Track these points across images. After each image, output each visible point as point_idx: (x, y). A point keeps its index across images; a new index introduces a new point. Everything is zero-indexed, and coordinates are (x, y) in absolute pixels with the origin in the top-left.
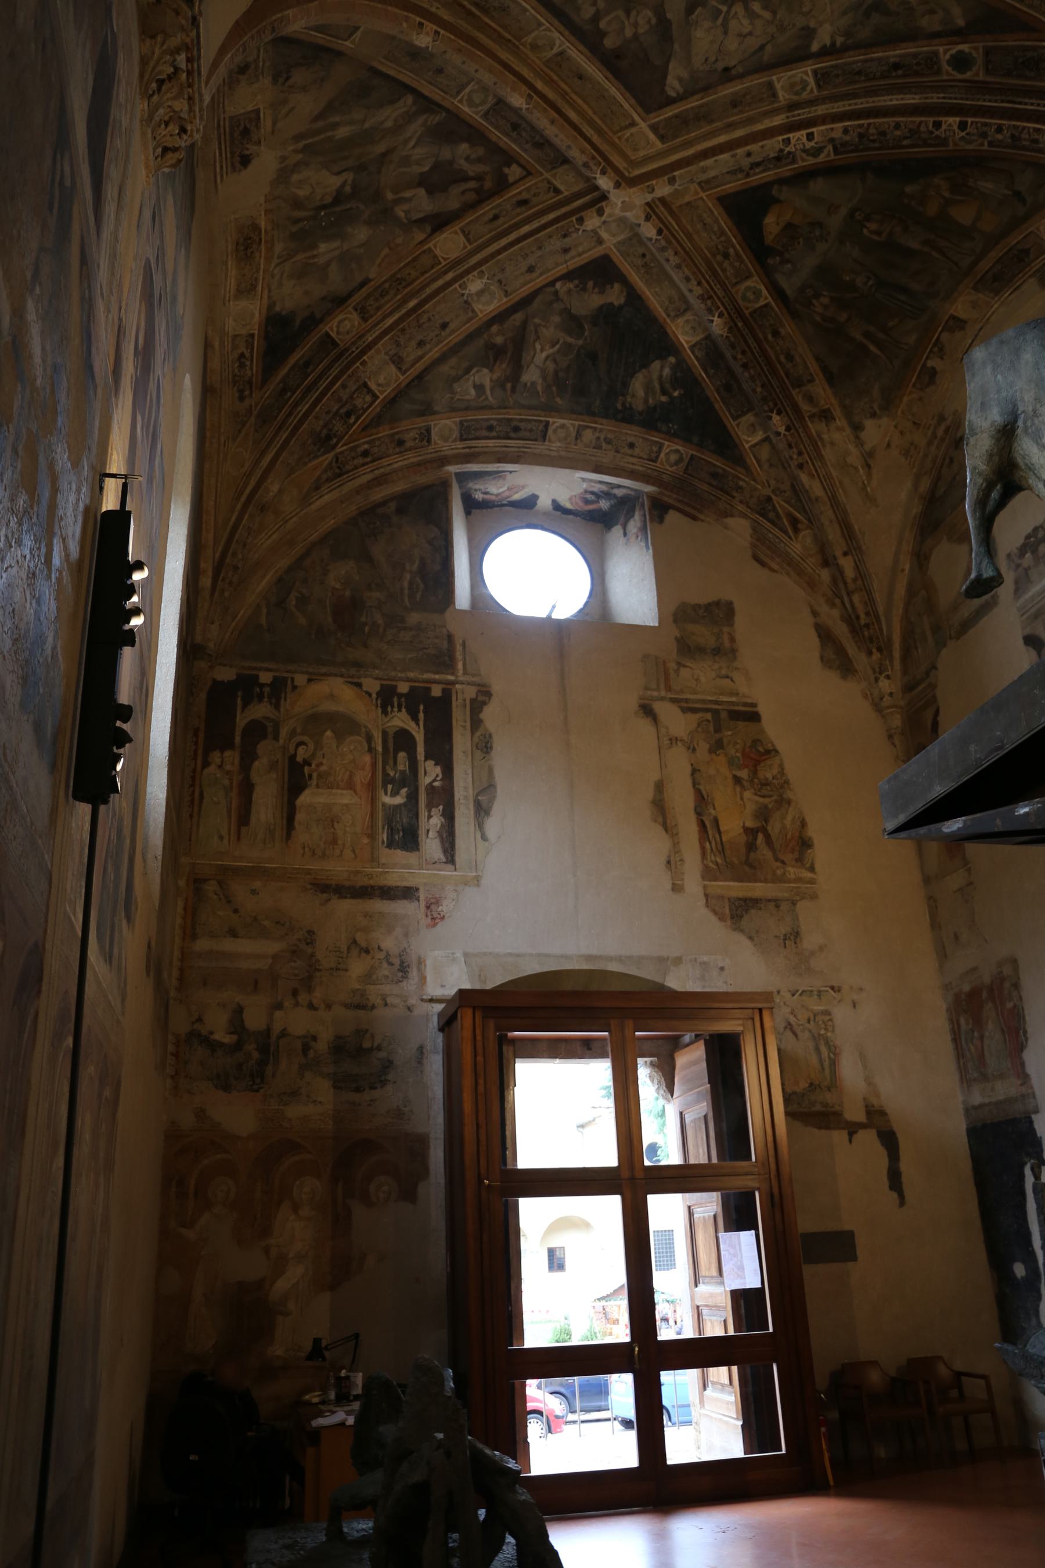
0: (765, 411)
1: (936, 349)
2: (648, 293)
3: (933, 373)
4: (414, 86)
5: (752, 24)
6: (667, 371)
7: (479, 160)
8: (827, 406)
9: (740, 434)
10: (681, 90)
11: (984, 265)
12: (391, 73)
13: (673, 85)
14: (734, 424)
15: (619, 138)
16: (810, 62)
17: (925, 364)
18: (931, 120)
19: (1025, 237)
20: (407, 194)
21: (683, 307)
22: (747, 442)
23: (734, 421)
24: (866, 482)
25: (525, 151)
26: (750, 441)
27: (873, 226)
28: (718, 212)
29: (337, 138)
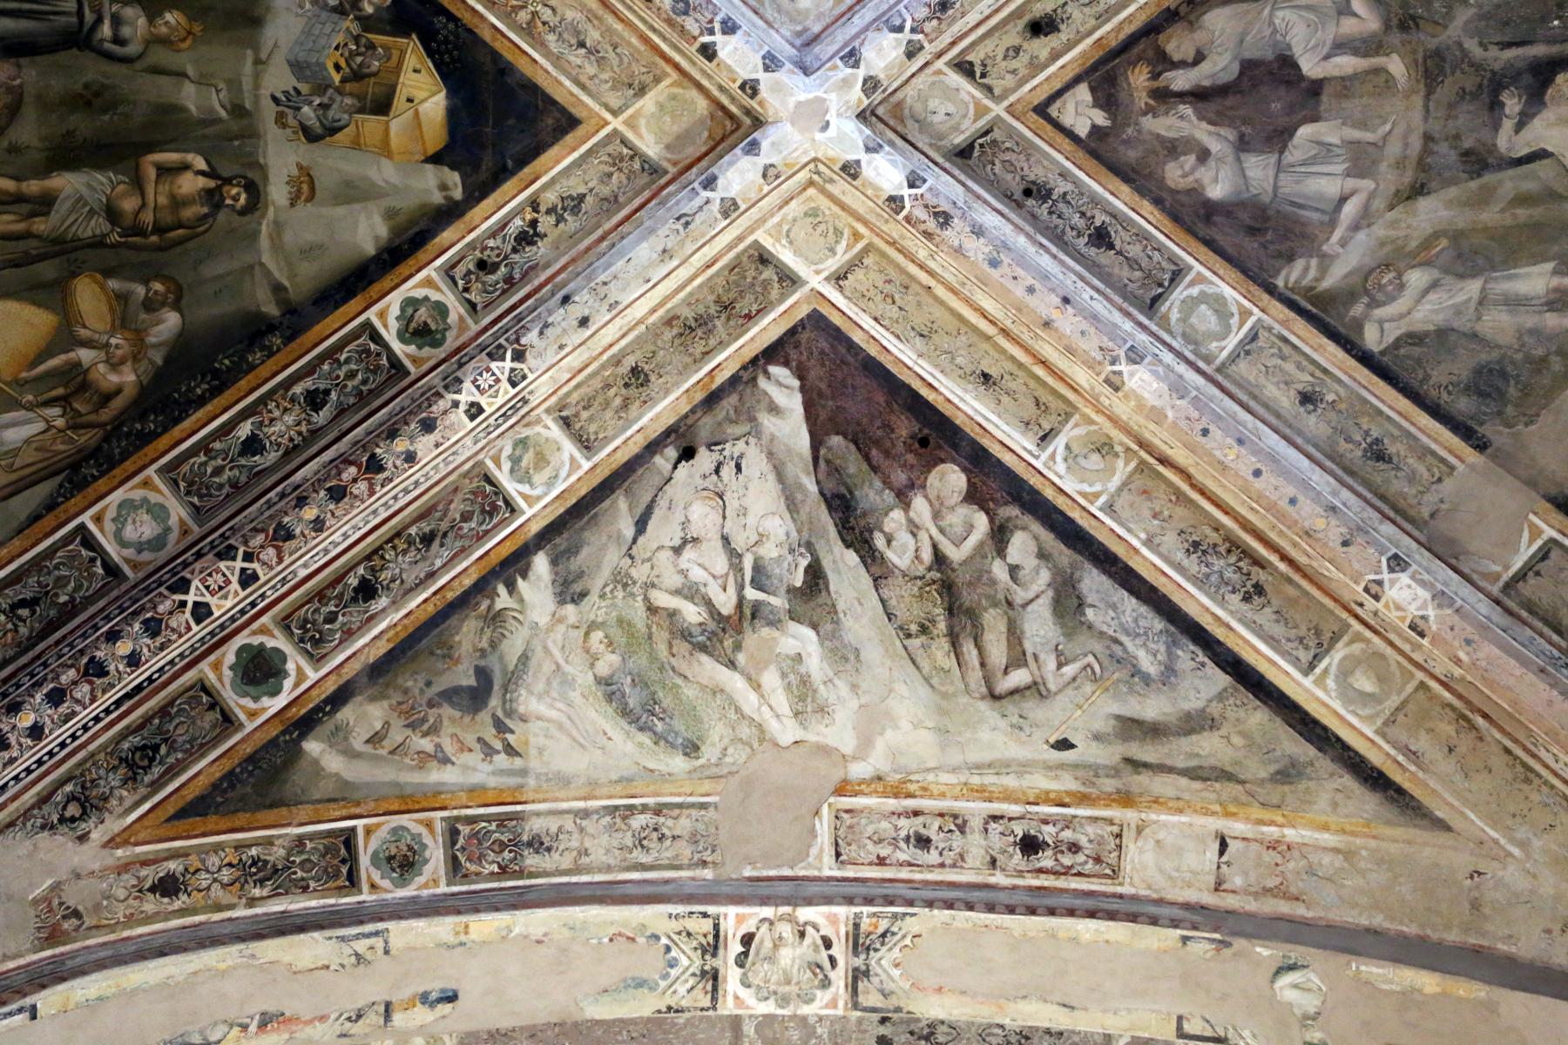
4: (1366, 371)
5: (684, 573)
7: (1173, 149)
10: (762, 382)
12: (1425, 420)
13: (782, 387)
15: (856, 236)
16: (535, 528)
20: (1346, 64)
25: (1064, 175)
27: (190, 184)
28: (562, 88)
29: (1550, 266)
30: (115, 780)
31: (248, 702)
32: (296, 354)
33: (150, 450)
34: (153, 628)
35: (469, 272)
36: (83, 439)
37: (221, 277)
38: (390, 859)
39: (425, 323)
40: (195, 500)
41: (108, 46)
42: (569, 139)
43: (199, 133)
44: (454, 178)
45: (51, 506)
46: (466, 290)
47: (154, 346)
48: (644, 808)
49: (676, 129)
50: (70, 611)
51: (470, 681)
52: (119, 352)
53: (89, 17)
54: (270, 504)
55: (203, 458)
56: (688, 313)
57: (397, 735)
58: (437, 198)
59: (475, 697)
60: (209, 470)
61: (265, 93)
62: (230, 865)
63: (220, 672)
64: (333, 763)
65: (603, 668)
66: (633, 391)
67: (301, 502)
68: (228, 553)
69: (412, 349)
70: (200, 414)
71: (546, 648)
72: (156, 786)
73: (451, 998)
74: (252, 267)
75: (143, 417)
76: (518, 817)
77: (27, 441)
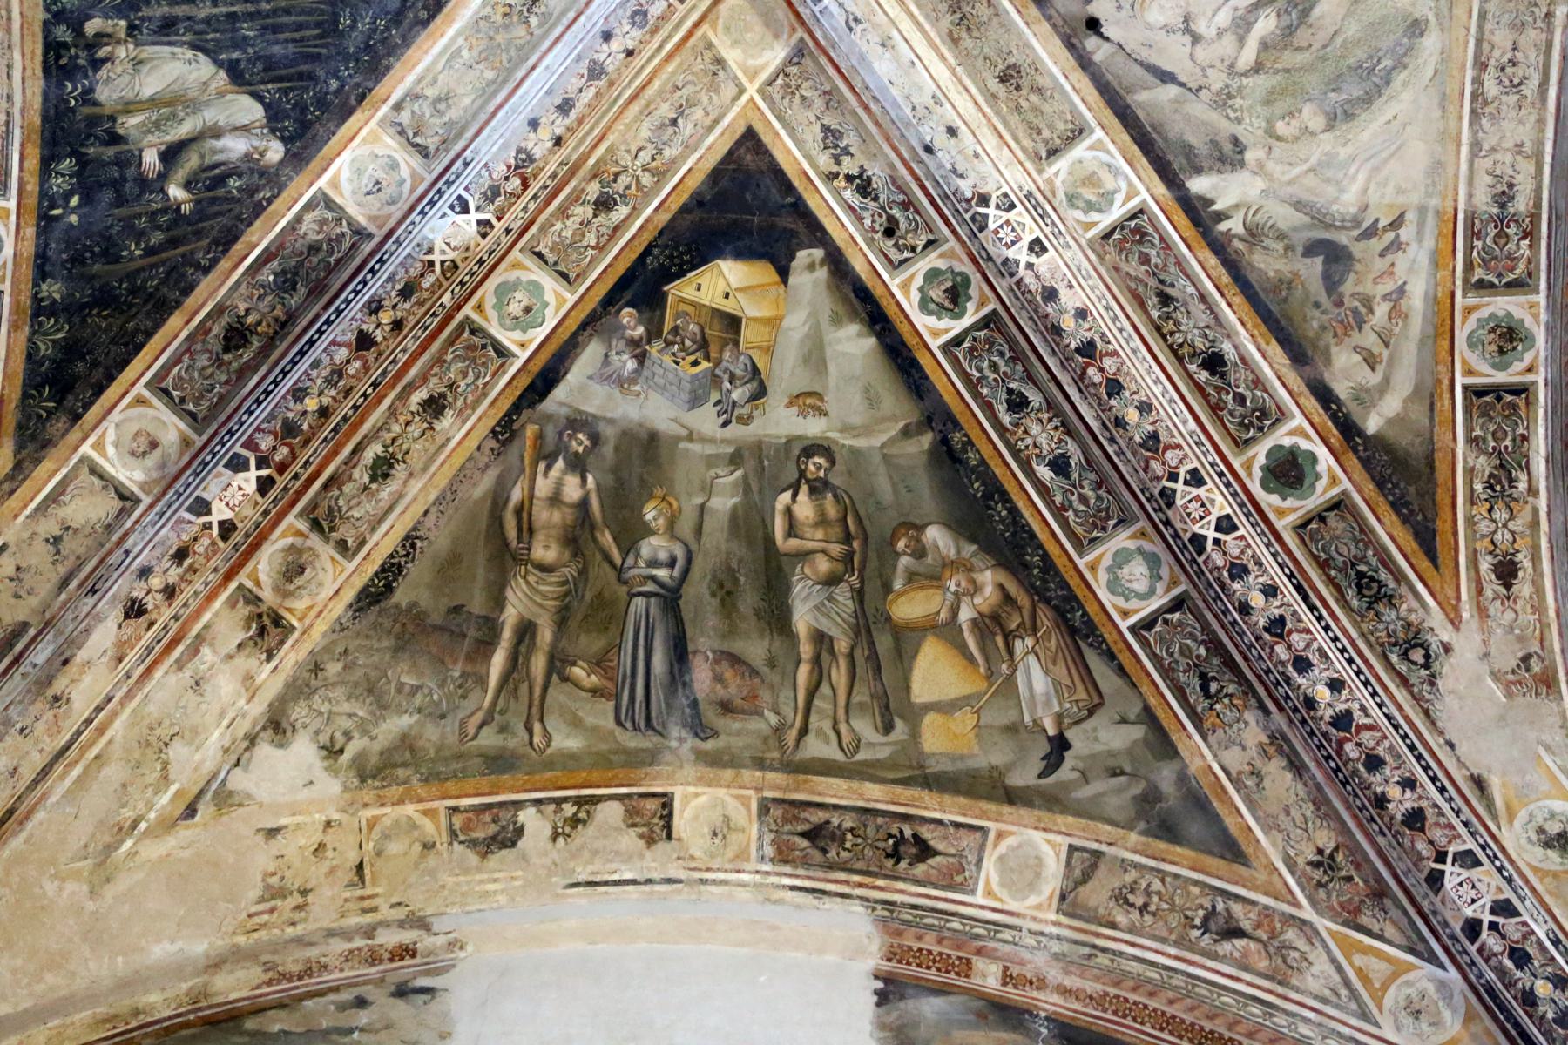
0: (250, 444)
1: (569, 809)
2: (451, 32)
3: (508, 838)
5: (1221, 33)
6: (235, 147)
8: (295, 623)
9: (116, 416)
11: (835, 790)
14: (140, 389)
16: (1161, 189)
17: (518, 805)
19: (957, 825)
21: (431, 143)
22: (99, 446)
23: (146, 386)
24: (143, 826)
26: (104, 455)
27: (805, 508)
30: (1389, 615)
31: (1321, 485)
32: (973, 421)
33: (1060, 562)
34: (1239, 571)
35: (896, 245)
36: (1046, 622)
37: (894, 485)
38: (1501, 351)
39: (945, 291)
40: (1111, 523)
41: (676, 573)
42: (767, 139)
43: (756, 497)
44: (803, 256)
45: (1111, 656)
46: (913, 249)
47: (959, 552)
48: (1477, 81)
49: (759, 28)
50: (1215, 645)
51: (1319, 260)
52: (963, 584)
53: (650, 587)
54: (1120, 453)
55: (1070, 513)
56: (947, 21)
57: (1369, 340)
58: (822, 273)
59: (1335, 258)
60: (1082, 508)
61: (720, 433)
62: (1490, 511)
63: (1287, 510)
64: (1392, 405)
65: (1316, 122)
66: (1025, 82)
67: (1120, 423)
68: (1168, 497)
69: (970, 306)
70: (1027, 513)
71: (1291, 182)
72: (1399, 577)
74: (885, 456)
75: (1027, 567)
76: (1471, 219)
77: (1046, 672)
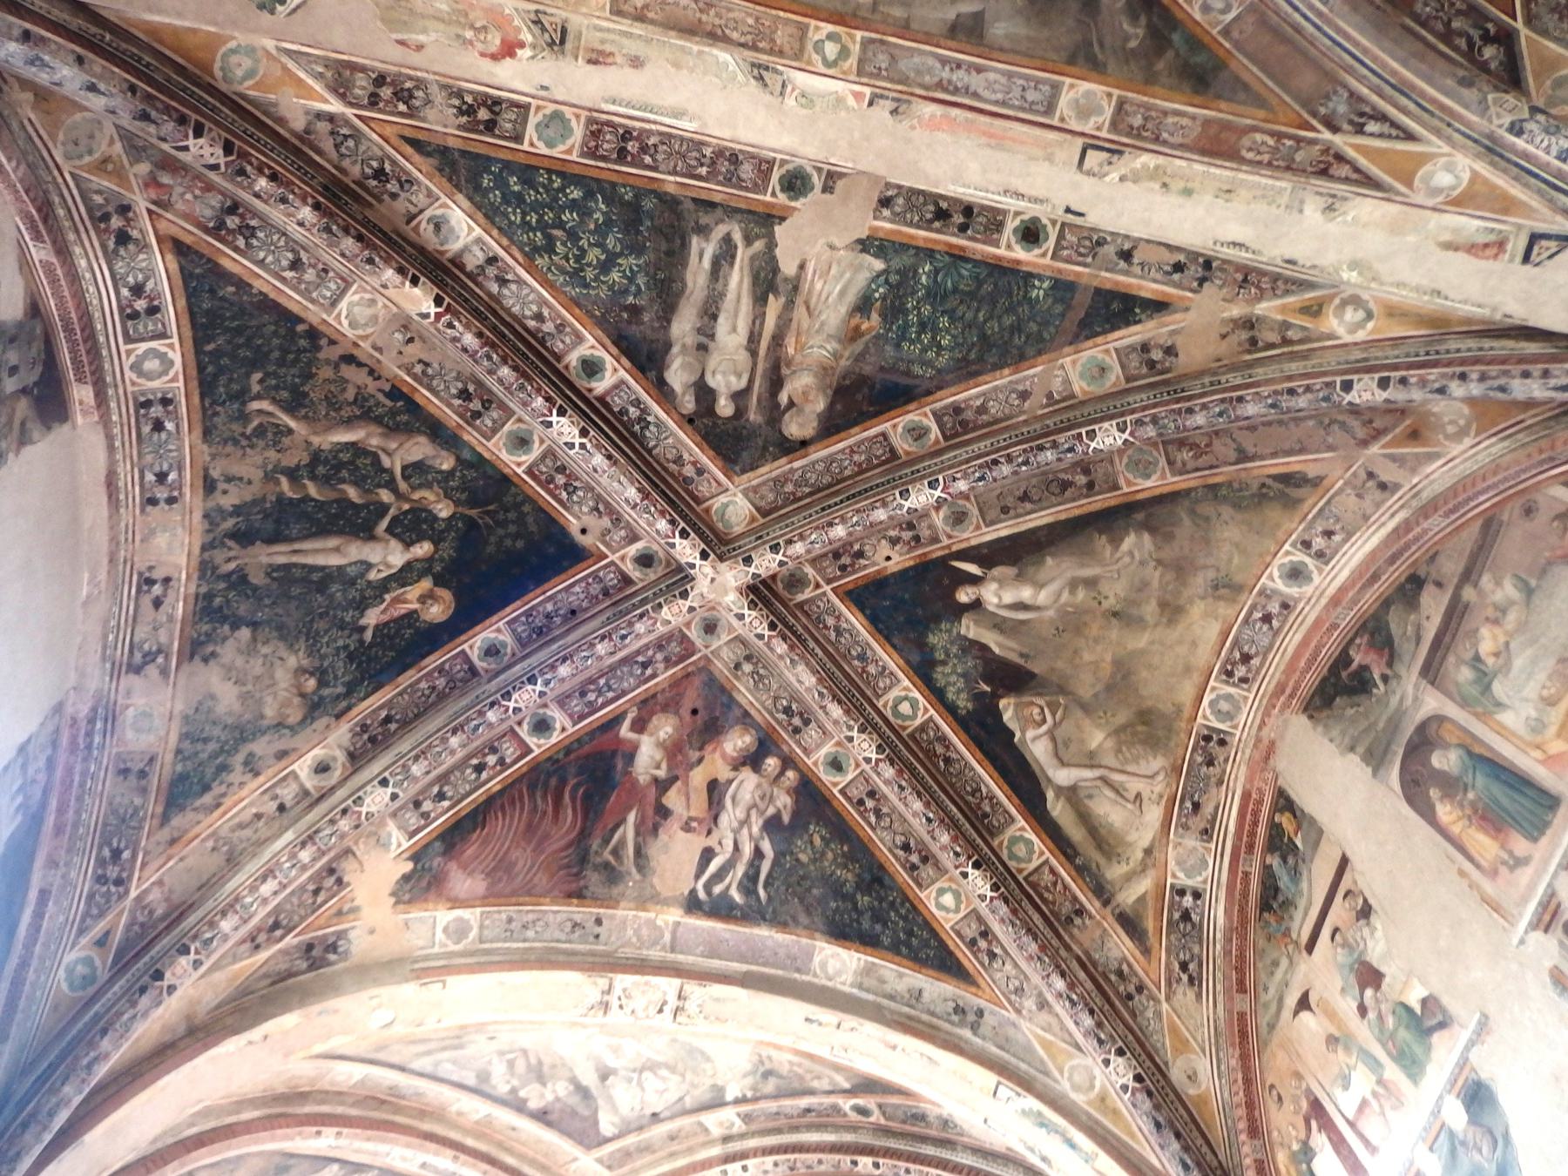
18: (848, 1159)
57: (808, 1077)
73: (807, 1020)
